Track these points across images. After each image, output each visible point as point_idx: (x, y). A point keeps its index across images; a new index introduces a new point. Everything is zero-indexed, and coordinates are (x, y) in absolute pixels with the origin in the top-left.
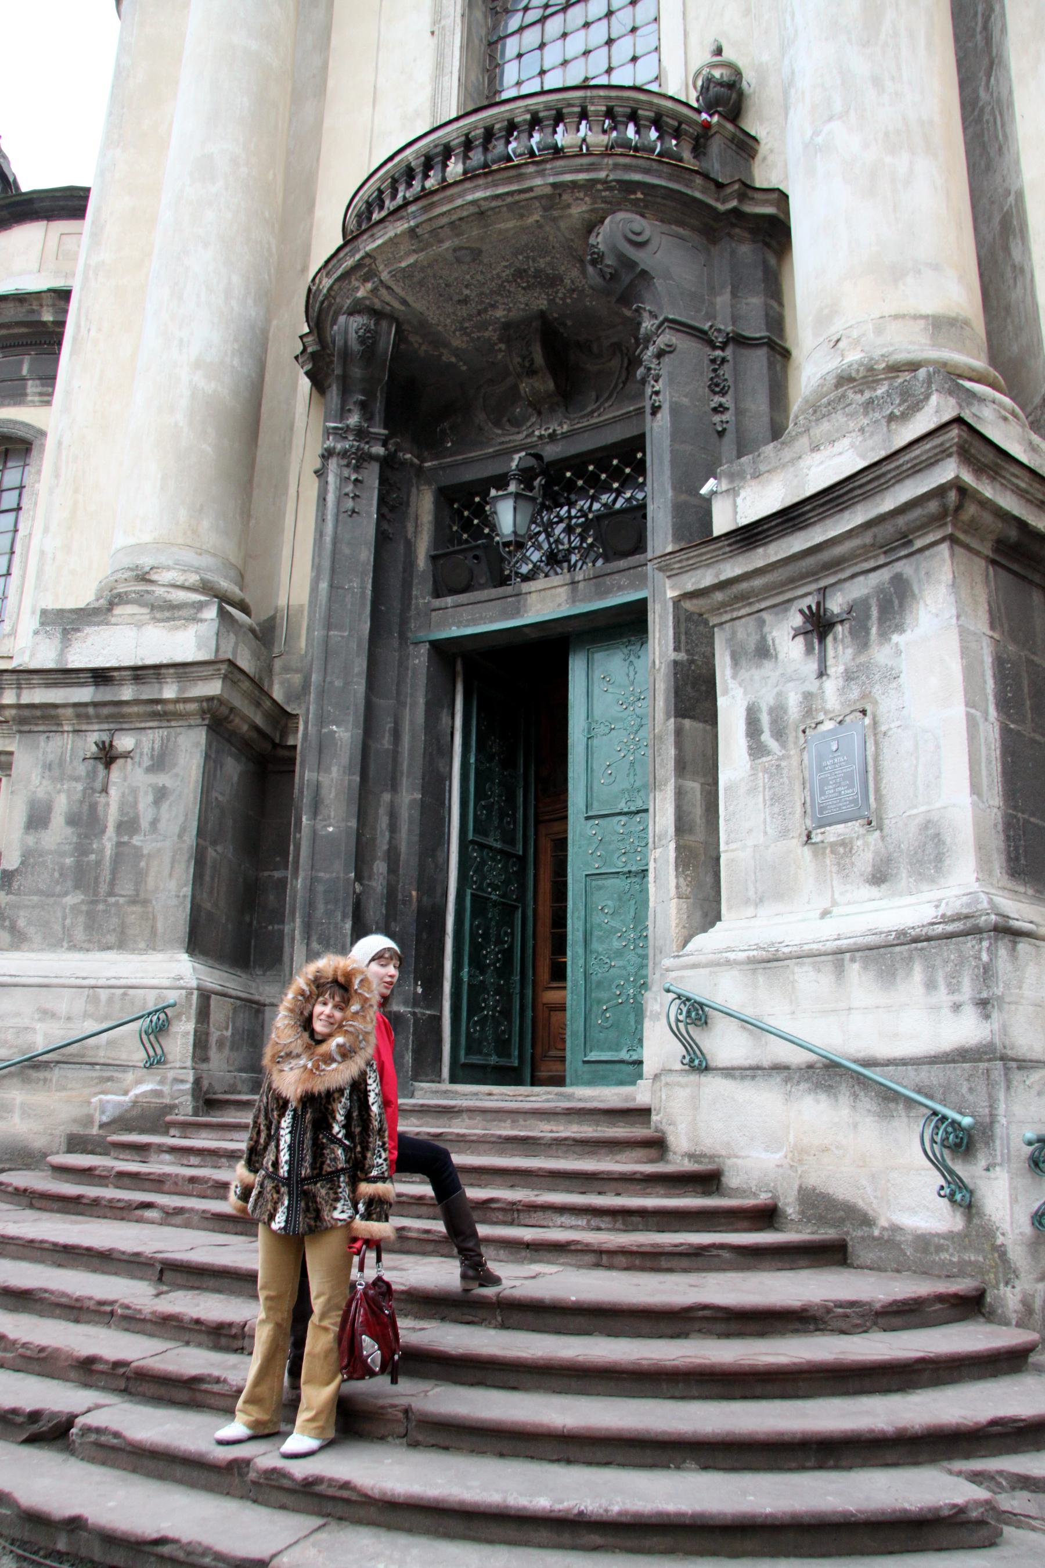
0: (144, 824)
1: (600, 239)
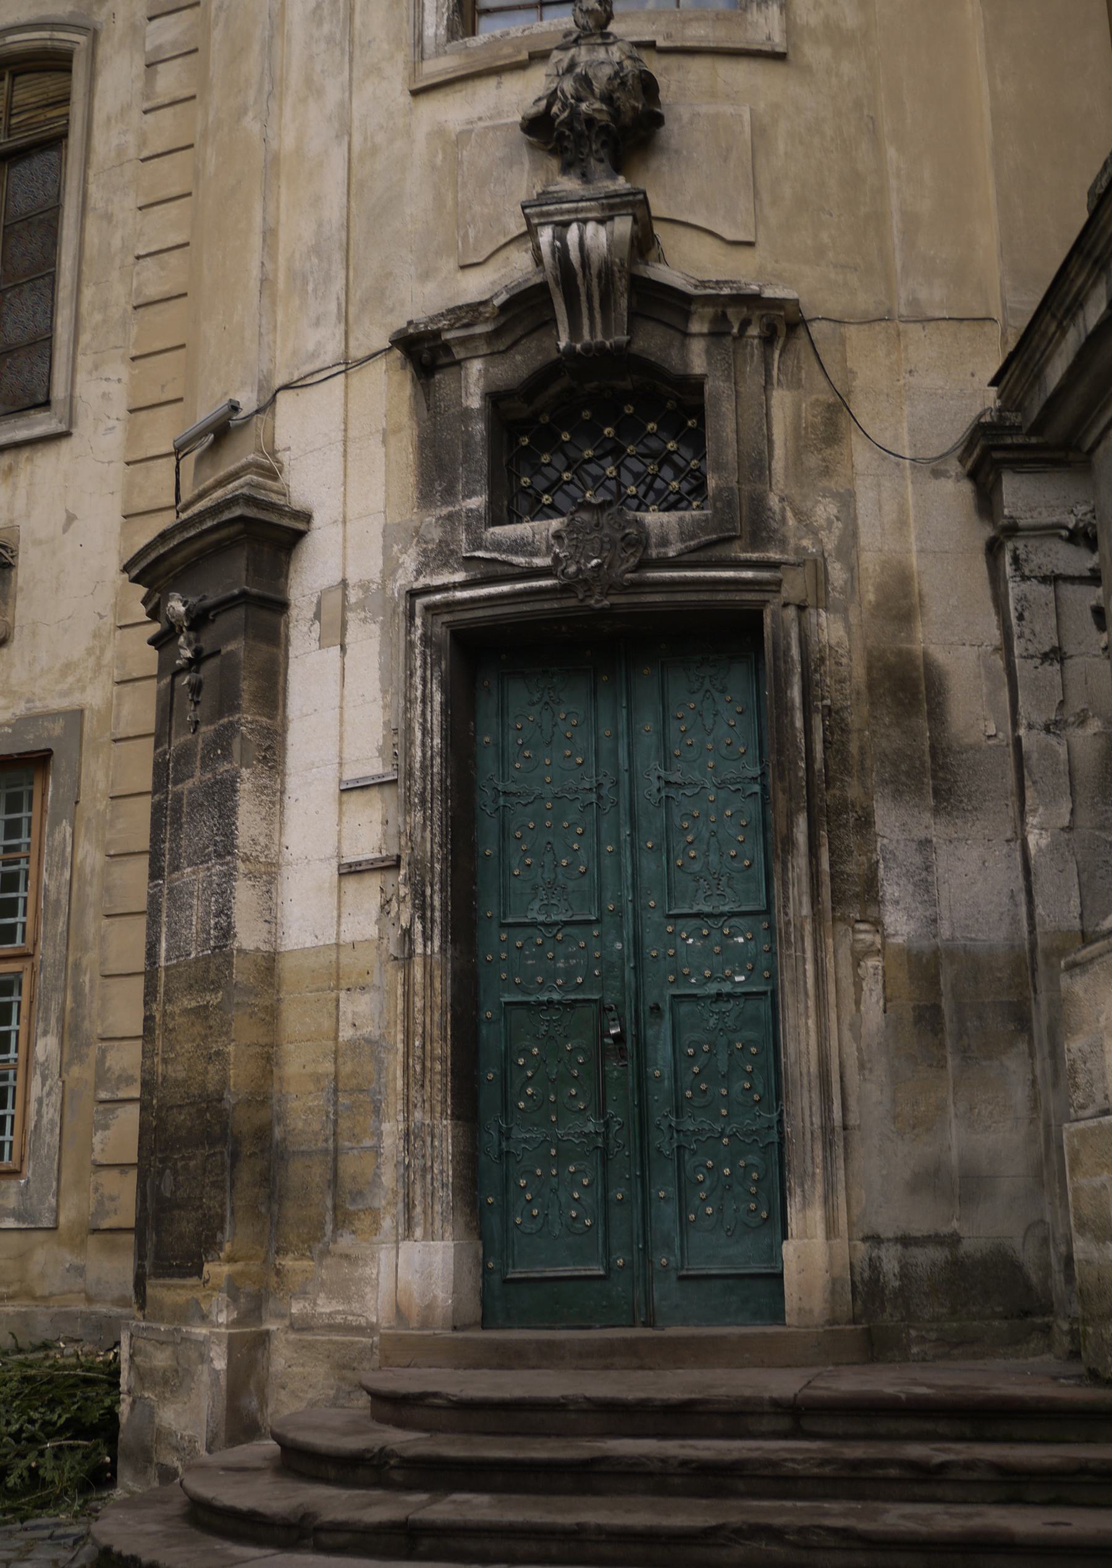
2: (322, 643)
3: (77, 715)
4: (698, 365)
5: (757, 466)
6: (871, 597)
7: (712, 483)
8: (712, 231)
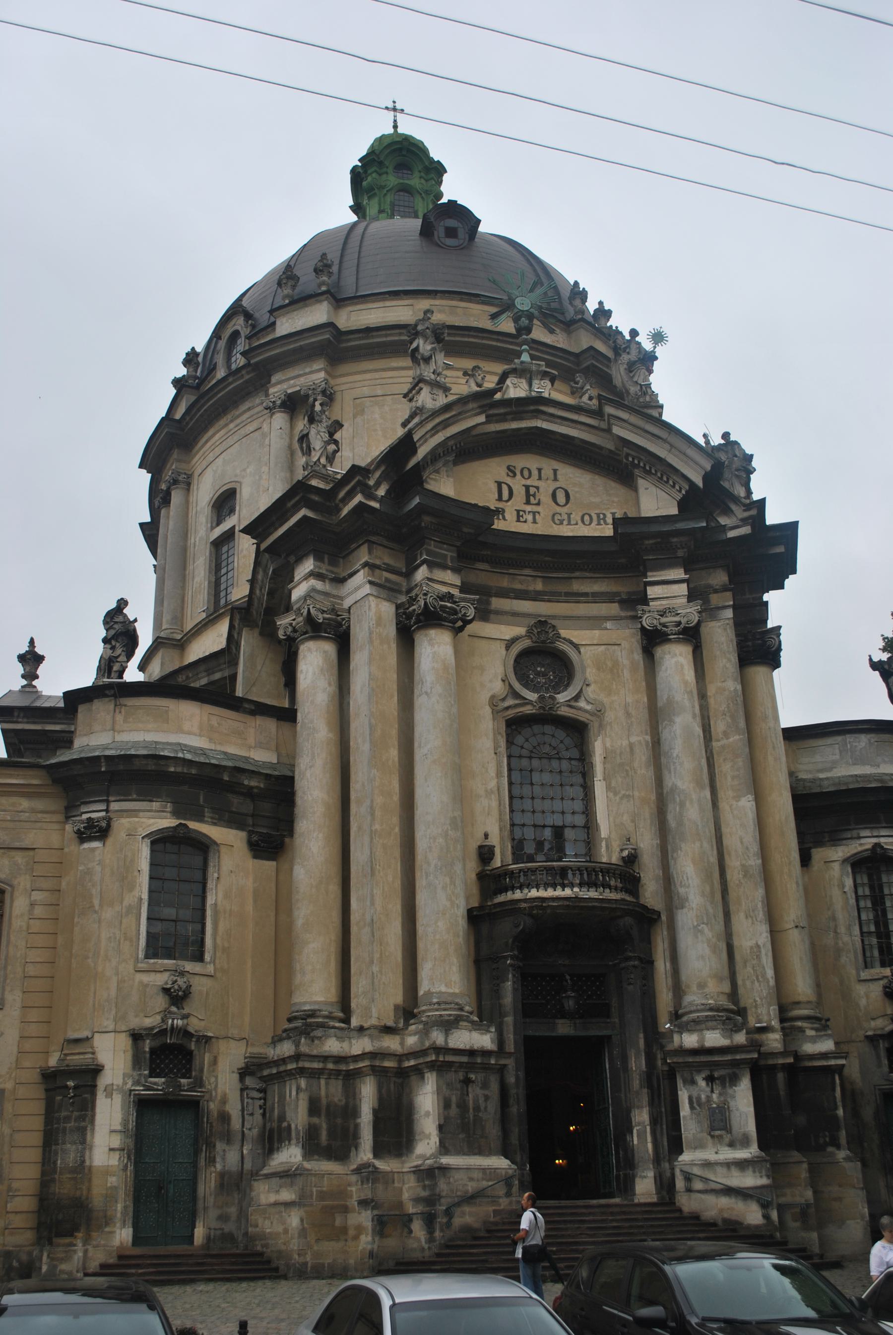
0: (482, 1108)
2: (106, 1097)
4: (193, 1047)
5: (202, 1070)
6: (219, 1098)
7: (193, 1074)
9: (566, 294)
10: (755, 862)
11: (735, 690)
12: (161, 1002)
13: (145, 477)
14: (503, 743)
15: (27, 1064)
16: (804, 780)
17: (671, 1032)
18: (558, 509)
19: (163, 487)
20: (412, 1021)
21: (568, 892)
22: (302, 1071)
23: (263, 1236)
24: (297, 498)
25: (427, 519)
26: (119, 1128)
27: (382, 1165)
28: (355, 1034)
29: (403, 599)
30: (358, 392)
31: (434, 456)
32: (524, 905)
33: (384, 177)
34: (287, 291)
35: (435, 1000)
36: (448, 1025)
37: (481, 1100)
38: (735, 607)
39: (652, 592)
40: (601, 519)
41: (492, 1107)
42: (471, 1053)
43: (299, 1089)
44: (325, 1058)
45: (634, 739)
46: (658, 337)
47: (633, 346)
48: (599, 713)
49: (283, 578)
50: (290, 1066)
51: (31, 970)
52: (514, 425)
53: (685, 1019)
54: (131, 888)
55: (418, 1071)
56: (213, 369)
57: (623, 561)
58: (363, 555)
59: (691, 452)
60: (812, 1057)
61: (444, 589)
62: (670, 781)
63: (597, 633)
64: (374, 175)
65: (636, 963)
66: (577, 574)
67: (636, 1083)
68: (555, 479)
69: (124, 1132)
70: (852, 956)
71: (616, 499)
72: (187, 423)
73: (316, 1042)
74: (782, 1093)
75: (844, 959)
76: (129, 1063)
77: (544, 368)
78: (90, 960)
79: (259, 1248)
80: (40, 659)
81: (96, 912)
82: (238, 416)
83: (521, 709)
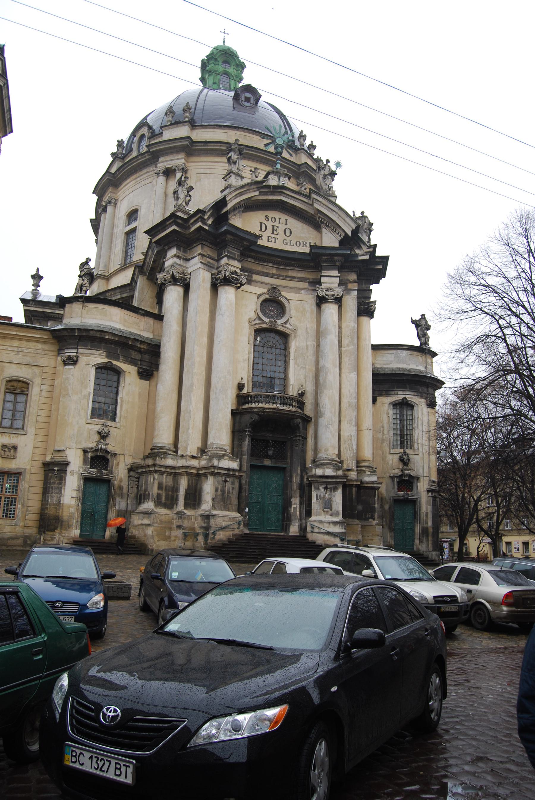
1: (296, 421)
3: (25, 469)
5: (112, 467)
8: (112, 445)
9: (297, 135)
10: (354, 401)
11: (354, 326)
12: (96, 437)
13: (95, 198)
14: (252, 339)
15: (37, 458)
16: (377, 368)
17: (312, 468)
18: (286, 238)
19: (104, 204)
20: (204, 455)
21: (275, 406)
22: (156, 471)
23: (134, 537)
24: (171, 221)
25: (229, 237)
26: (76, 488)
27: (188, 512)
28: (180, 458)
29: (214, 271)
30: (198, 171)
31: (234, 208)
32: (256, 410)
33: (217, 66)
34: (170, 118)
35: (215, 447)
36: (220, 457)
37: (231, 489)
38: (358, 290)
39: (323, 280)
40: (304, 244)
41: (236, 492)
42: (229, 470)
43: (154, 479)
44: (166, 467)
45: (308, 343)
46: (338, 165)
47: (327, 167)
48: (295, 330)
49: (161, 255)
50: (151, 469)
51: (40, 419)
52: (271, 197)
53: (318, 463)
54: (86, 388)
55: (205, 475)
56: (131, 150)
57: (312, 264)
58: (199, 250)
59: (348, 219)
60: (368, 483)
61: (234, 269)
62: (321, 363)
63: (297, 295)
64: (212, 65)
65: (300, 438)
66: (292, 268)
67: (295, 487)
68: (286, 224)
69: (78, 490)
70: (388, 443)
71: (312, 236)
72: (117, 175)
73: (163, 460)
74: (354, 496)
75: (385, 444)
76: (82, 462)
77: (286, 172)
78: (66, 417)
79: (133, 542)
80: (41, 278)
81: (70, 397)
82: (142, 175)
83: (261, 325)
